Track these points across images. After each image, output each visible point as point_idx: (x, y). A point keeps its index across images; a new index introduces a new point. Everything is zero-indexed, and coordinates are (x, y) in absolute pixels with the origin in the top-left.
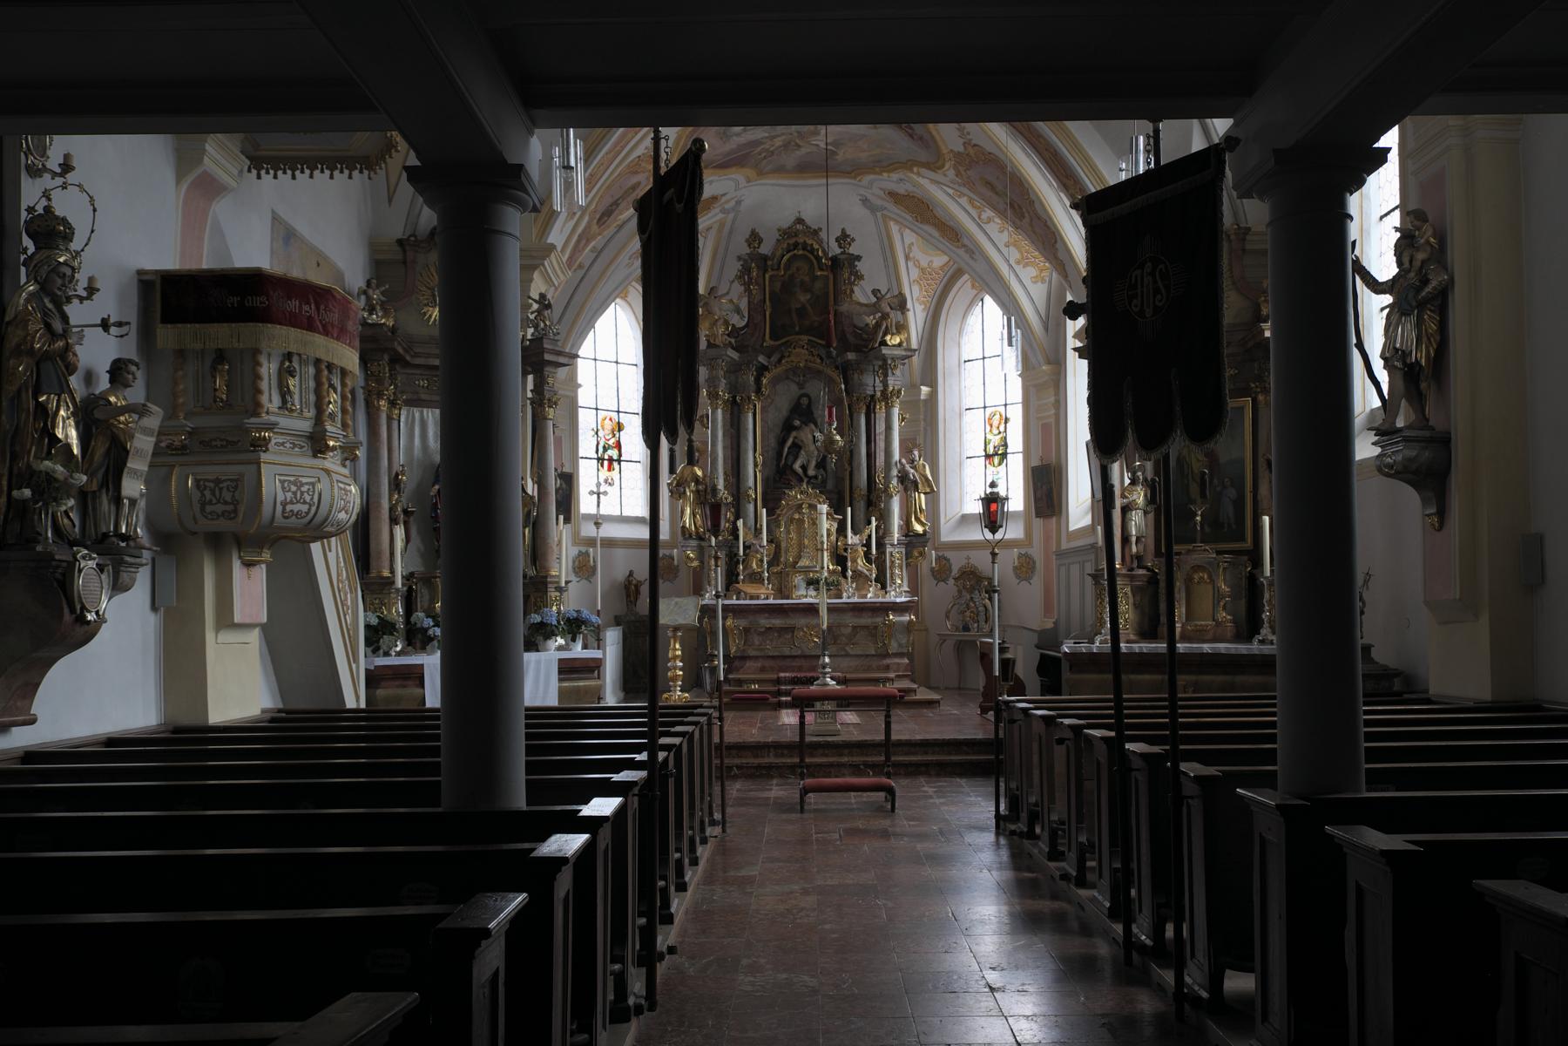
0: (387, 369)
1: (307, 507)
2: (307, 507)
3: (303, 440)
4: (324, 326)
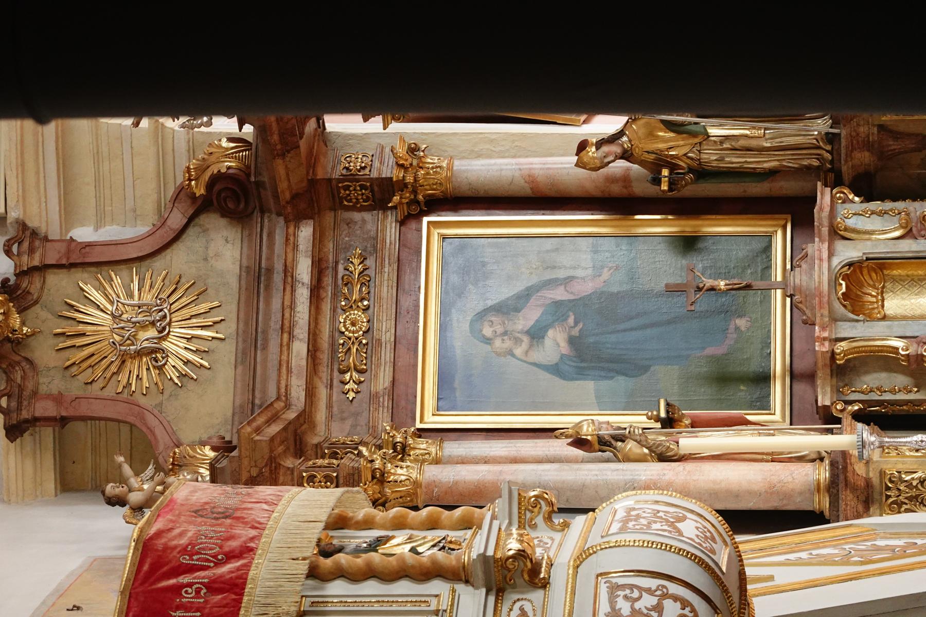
0: (320, 462)
1: (668, 604)
2: (668, 604)
3: (505, 610)
4: (231, 556)
